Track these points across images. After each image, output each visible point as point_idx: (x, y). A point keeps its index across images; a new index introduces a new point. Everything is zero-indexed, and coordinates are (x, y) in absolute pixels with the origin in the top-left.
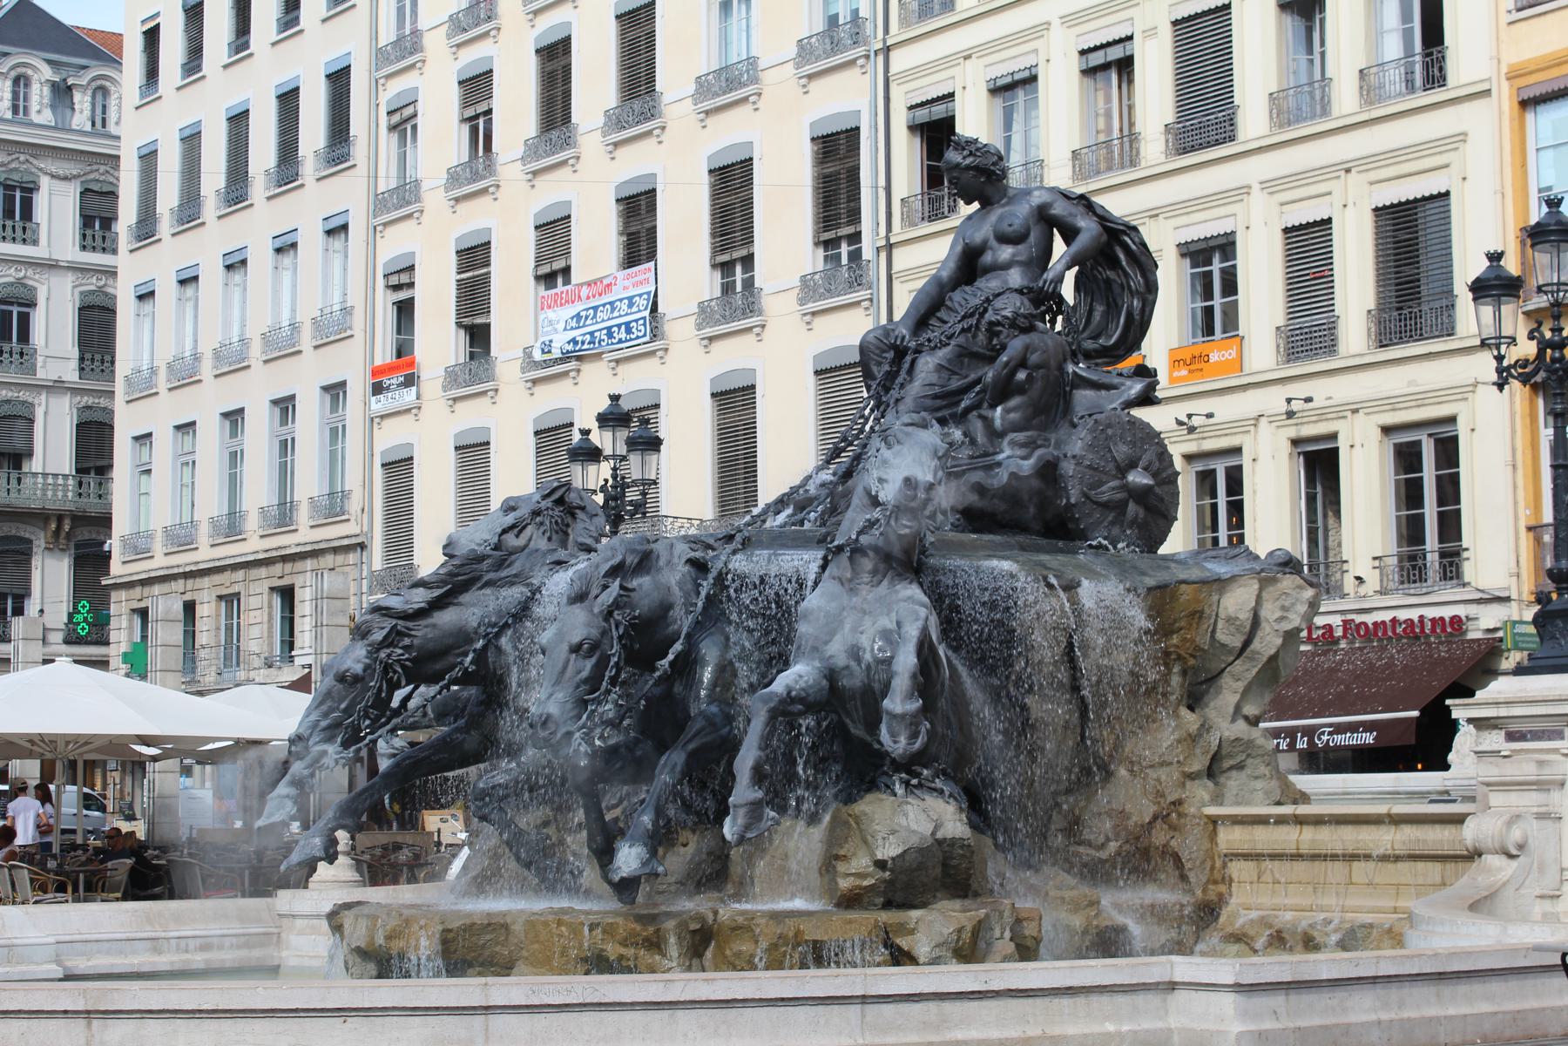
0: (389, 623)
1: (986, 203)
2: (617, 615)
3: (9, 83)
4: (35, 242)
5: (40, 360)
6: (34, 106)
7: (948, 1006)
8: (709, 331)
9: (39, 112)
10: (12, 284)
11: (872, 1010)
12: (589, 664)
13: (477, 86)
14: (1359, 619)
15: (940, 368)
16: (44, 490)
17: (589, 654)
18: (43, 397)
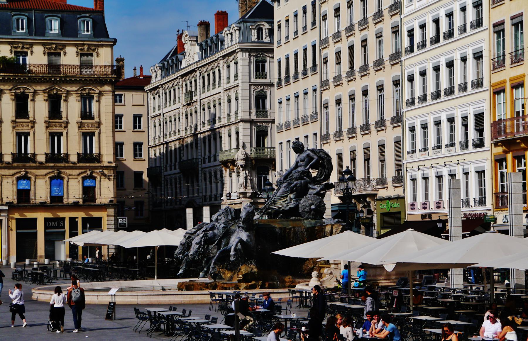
0: (188, 235)
1: (301, 153)
2: (203, 238)
3: (256, 31)
4: (266, 78)
5: (268, 114)
6: (264, 37)
7: (193, 296)
8: (378, 129)
9: (265, 38)
10: (259, 91)
11: (183, 296)
12: (198, 246)
13: (338, 54)
14: (471, 213)
15: (285, 187)
16: (270, 152)
17: (198, 244)
18: (270, 124)
